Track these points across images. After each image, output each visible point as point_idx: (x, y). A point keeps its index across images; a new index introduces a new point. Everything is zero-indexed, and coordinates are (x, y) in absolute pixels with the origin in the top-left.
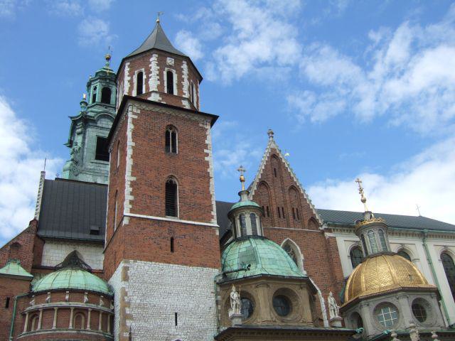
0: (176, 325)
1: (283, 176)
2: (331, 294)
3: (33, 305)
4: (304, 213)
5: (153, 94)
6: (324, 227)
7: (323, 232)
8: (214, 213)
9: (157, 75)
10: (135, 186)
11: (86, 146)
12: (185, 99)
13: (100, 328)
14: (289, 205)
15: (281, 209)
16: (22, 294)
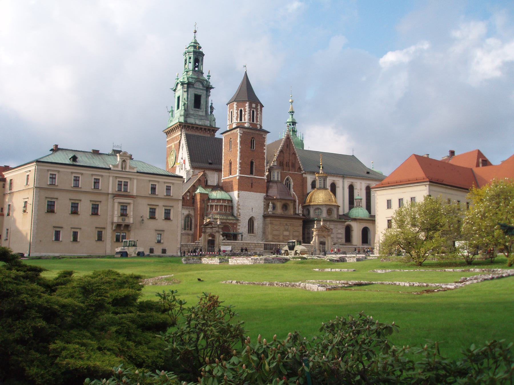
5: (247, 123)
6: (304, 172)
7: (302, 174)
11: (189, 99)
14: (291, 162)
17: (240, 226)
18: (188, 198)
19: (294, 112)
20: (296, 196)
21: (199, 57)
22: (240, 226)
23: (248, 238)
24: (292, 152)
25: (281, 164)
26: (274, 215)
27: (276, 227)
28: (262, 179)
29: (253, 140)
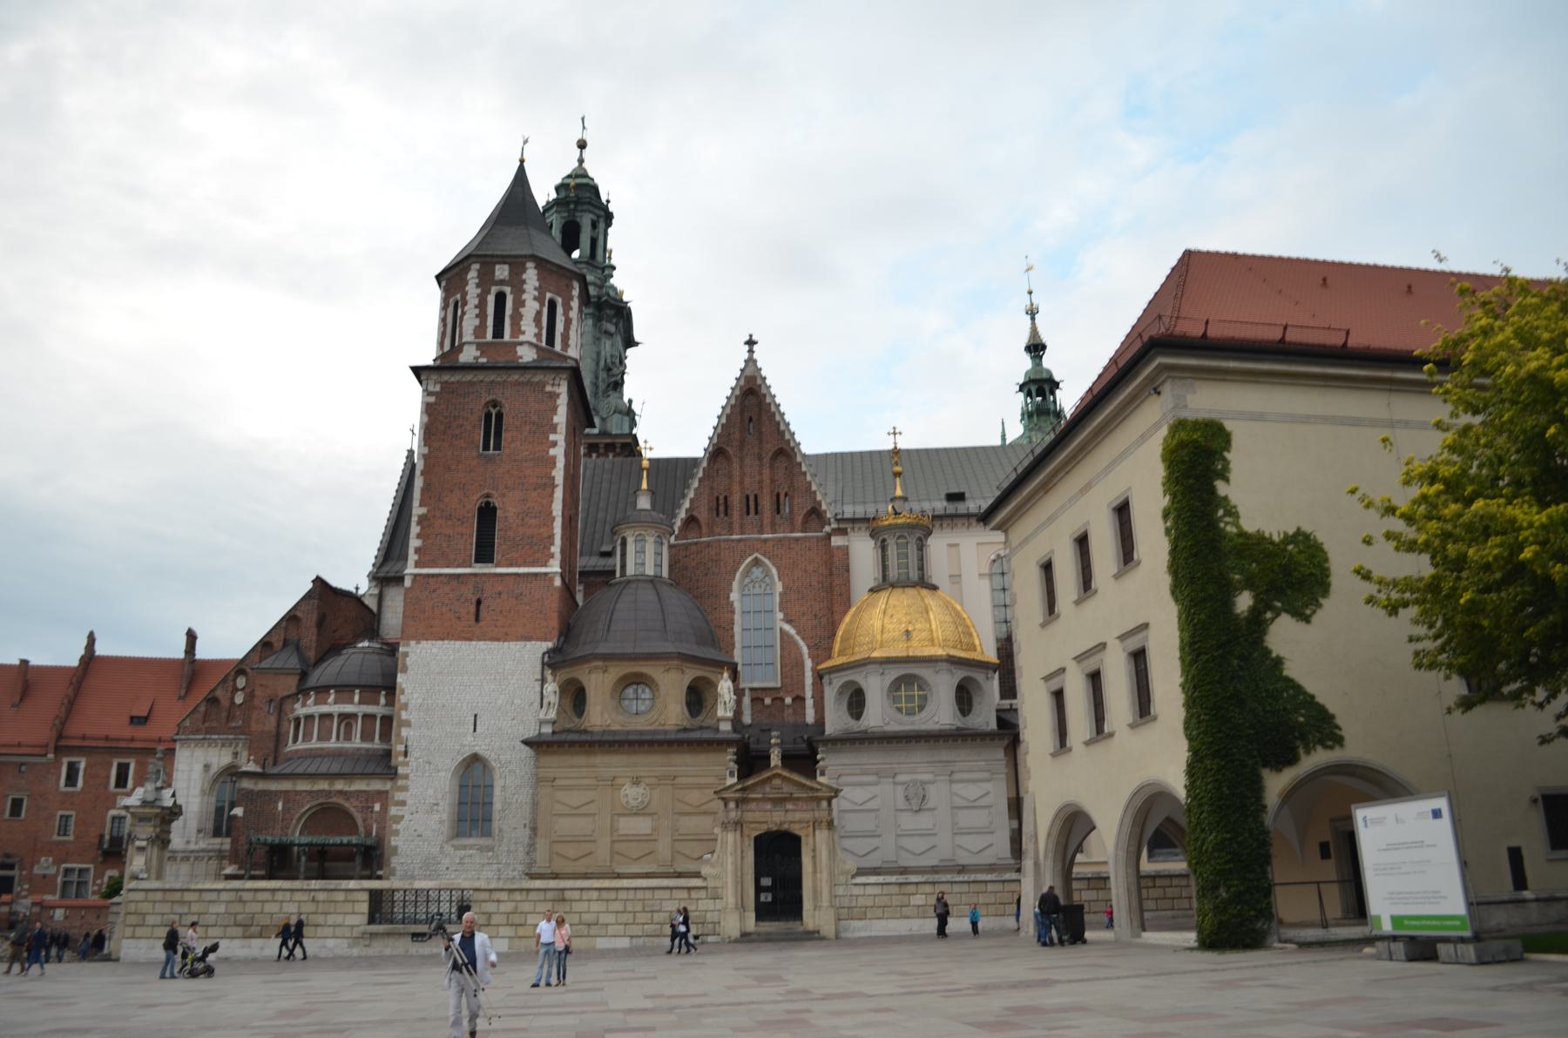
0: (475, 730)
1: (763, 430)
2: (726, 675)
3: (301, 710)
4: (796, 501)
5: (466, 348)
6: (834, 526)
7: (829, 536)
8: (556, 549)
9: (476, 307)
10: (425, 523)
12: (521, 344)
13: (377, 737)
14: (766, 491)
15: (752, 498)
16: (289, 693)
17: (403, 803)
18: (239, 699)
19: (1044, 347)
20: (802, 643)
21: (578, 214)
22: (403, 803)
23: (446, 861)
24: (770, 448)
25: (722, 508)
26: (556, 738)
27: (574, 798)
28: (536, 575)
29: (494, 412)
